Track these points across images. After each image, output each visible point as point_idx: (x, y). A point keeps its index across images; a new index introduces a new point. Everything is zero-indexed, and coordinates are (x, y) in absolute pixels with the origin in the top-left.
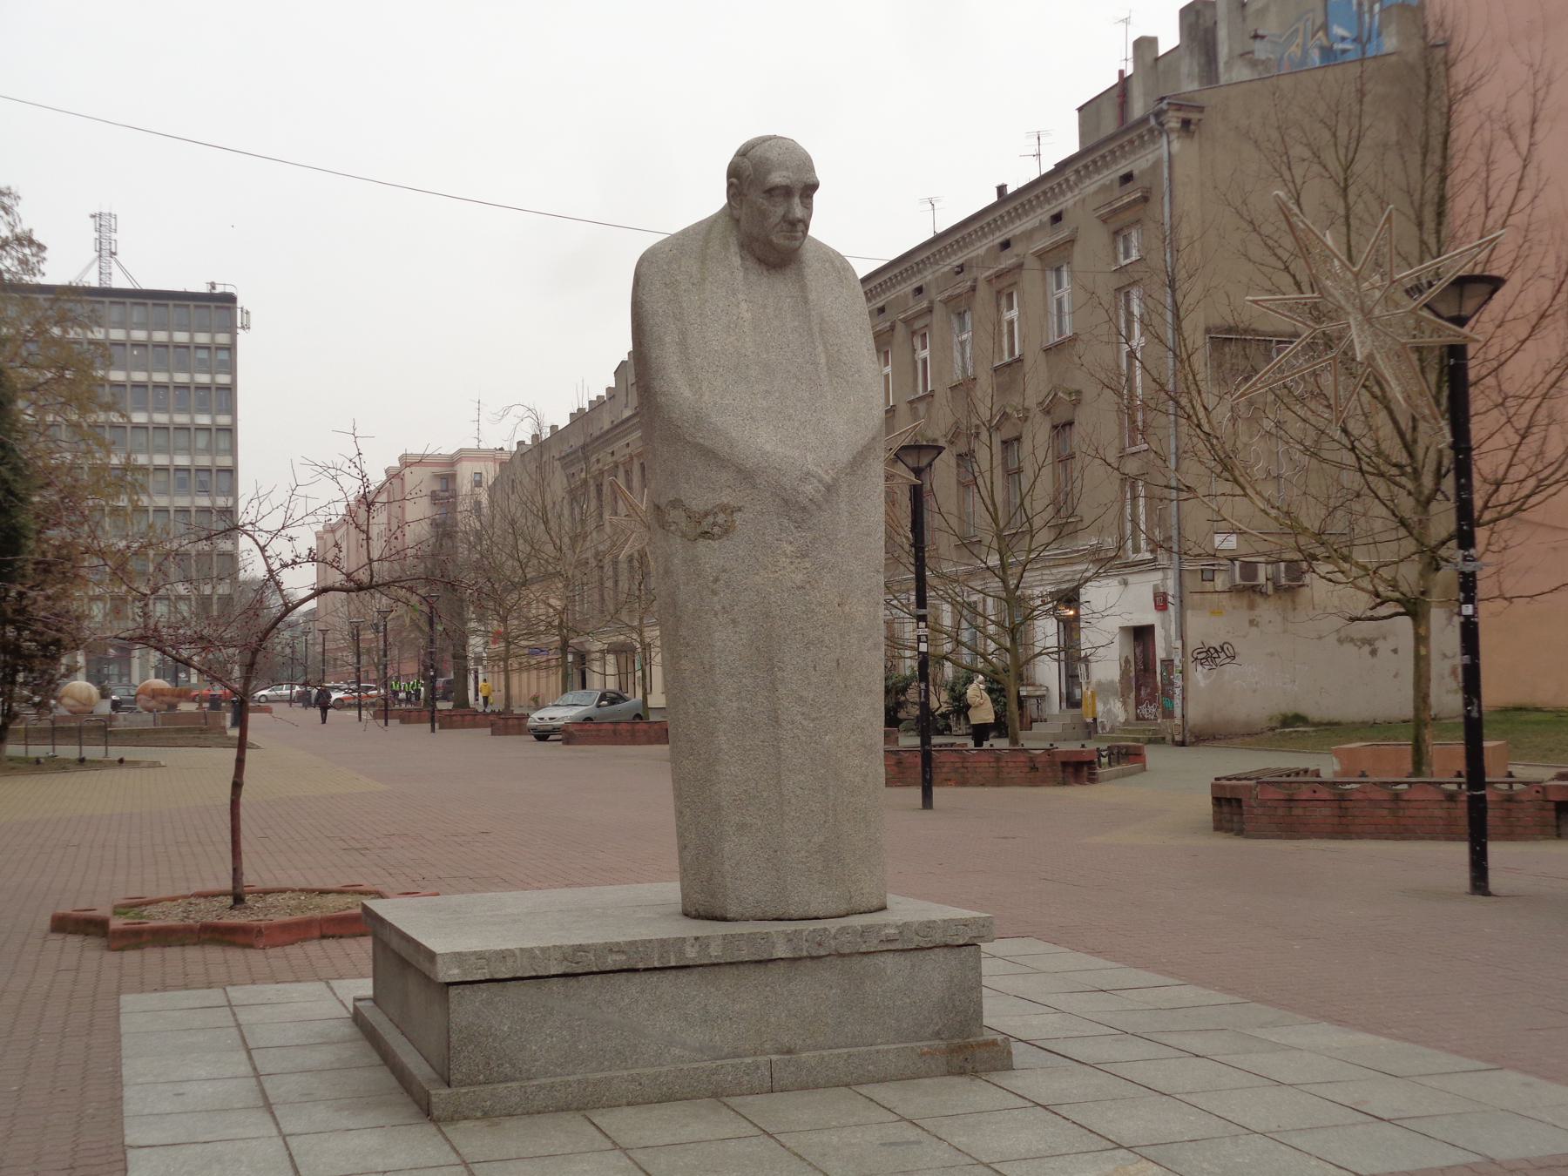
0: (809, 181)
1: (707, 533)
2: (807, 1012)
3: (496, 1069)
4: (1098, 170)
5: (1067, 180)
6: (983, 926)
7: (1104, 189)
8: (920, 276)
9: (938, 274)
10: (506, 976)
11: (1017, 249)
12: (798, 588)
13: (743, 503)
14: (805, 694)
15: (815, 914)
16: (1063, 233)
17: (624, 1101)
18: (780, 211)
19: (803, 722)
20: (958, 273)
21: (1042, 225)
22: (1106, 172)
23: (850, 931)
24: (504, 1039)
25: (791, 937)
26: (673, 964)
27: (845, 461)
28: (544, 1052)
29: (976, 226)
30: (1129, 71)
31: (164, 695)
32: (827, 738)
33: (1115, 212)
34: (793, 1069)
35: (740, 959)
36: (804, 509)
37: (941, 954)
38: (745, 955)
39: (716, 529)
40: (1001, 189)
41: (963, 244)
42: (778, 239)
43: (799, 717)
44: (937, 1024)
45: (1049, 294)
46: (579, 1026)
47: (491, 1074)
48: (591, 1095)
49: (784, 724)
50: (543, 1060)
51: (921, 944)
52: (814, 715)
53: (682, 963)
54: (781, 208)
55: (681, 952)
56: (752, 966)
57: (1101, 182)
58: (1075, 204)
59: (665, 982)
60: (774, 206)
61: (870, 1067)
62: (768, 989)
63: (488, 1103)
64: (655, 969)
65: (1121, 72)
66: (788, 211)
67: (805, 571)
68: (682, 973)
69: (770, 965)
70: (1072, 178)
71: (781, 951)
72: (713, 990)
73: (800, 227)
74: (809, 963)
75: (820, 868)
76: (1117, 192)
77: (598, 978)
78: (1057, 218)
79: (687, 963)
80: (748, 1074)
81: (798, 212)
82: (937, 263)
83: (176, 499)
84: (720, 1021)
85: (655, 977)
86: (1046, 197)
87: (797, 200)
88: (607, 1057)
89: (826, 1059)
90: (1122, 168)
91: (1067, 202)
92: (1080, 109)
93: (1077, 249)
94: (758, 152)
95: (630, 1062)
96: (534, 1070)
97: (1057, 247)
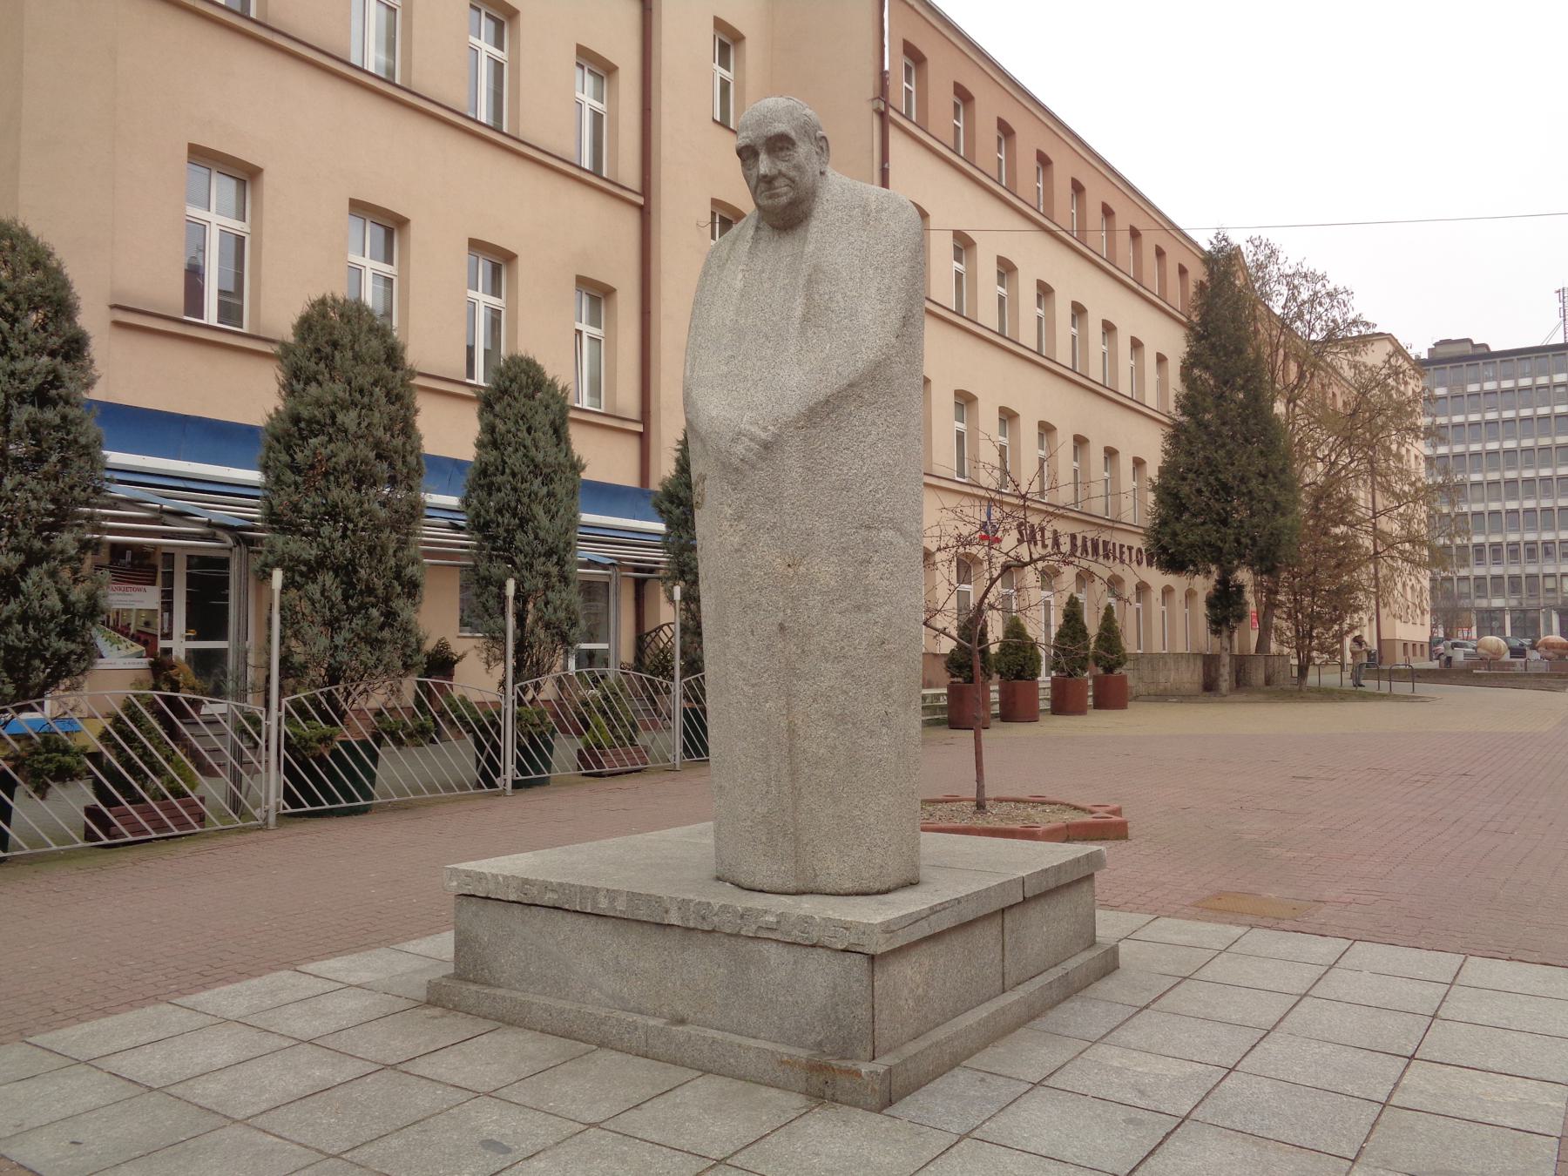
6: (864, 933)
15: (760, 887)
17: (539, 1027)
19: (746, 688)
26: (589, 911)
31: (1554, 648)
34: (664, 1039)
35: (638, 918)
36: (737, 469)
37: (825, 956)
38: (642, 914)
44: (819, 1033)
46: (531, 950)
49: (731, 689)
51: (799, 940)
52: (754, 682)
53: (594, 912)
55: (595, 902)
56: (654, 927)
59: (588, 927)
61: (732, 1060)
62: (666, 953)
64: (577, 912)
68: (600, 921)
69: (668, 930)
75: (764, 840)
77: (543, 911)
79: (598, 912)
80: (629, 1032)
83: (1542, 501)
85: (582, 920)
87: (763, 157)
89: (693, 1038)
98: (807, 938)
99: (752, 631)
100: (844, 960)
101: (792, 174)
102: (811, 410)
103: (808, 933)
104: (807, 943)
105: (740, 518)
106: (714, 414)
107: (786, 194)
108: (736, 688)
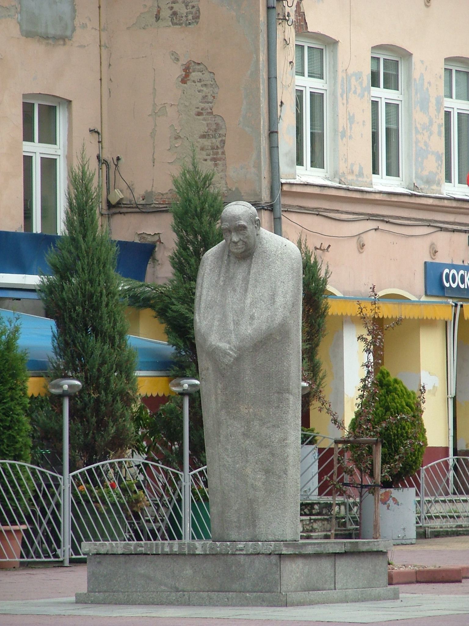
12: (224, 402)
19: (227, 459)
32: (237, 466)
43: (226, 456)
63: (93, 598)
74: (211, 557)
80: (181, 598)
99: (231, 435)
100: (270, 558)
101: (245, 240)
102: (255, 345)
106: (213, 343)
107: (243, 248)
108: (223, 458)
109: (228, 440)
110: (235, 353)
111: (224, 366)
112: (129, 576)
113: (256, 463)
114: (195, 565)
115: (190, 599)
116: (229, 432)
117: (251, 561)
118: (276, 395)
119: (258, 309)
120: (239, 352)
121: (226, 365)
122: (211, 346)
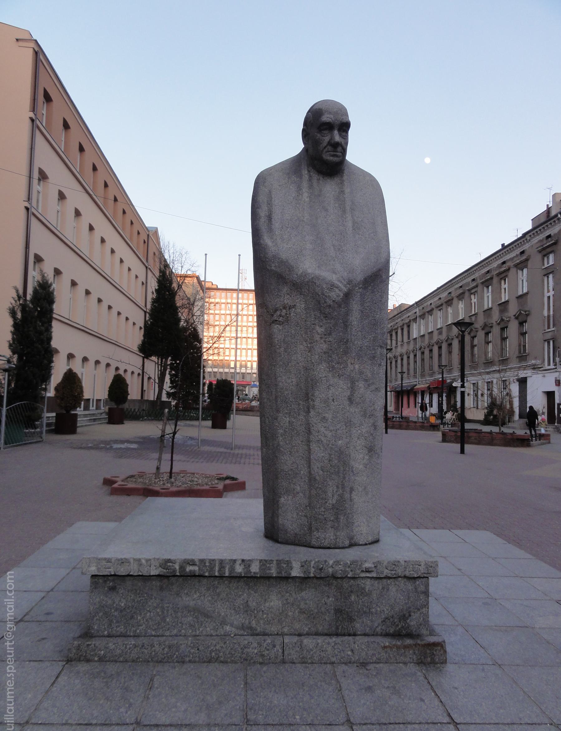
0: (344, 121)
1: (276, 321)
2: (312, 611)
3: (115, 629)
4: (538, 235)
5: (526, 239)
7: (541, 241)
8: (474, 275)
9: (480, 274)
10: (124, 574)
11: (508, 264)
12: (325, 353)
13: (295, 303)
14: (327, 415)
16: (524, 257)
17: (187, 659)
18: (327, 139)
19: (325, 432)
20: (487, 273)
21: (517, 255)
22: (541, 235)
23: (342, 563)
24: (121, 611)
25: (303, 564)
27: (358, 280)
28: (145, 621)
29: (494, 257)
30: (550, 205)
32: (340, 442)
33: (544, 249)
37: (403, 582)
39: (281, 319)
40: (503, 245)
41: (489, 264)
42: (327, 157)
45: (519, 278)
46: (168, 607)
47: (112, 631)
48: (167, 654)
50: (144, 626)
51: (389, 575)
54: (327, 138)
55: (232, 569)
57: (539, 239)
58: (529, 247)
60: (323, 136)
62: (288, 594)
63: (102, 652)
65: (548, 205)
66: (332, 138)
67: (329, 343)
70: (528, 238)
71: (296, 572)
72: (252, 592)
73: (339, 149)
76: (545, 241)
78: (522, 253)
80: (268, 650)
81: (337, 138)
82: (480, 270)
84: (256, 612)
86: (519, 246)
87: (336, 132)
88: (184, 627)
90: (547, 233)
91: (526, 247)
92: (532, 220)
93: (529, 262)
94: (315, 108)
95: (198, 632)
96: (138, 631)
97: (521, 262)
98: (395, 574)
99: (333, 400)
103: (396, 571)
104: (394, 576)
105: (330, 334)
106: (310, 271)
109: (328, 406)
110: (345, 286)
111: (329, 302)
112: (168, 611)
113: (358, 438)
114: (287, 592)
115: (286, 653)
116: (330, 395)
117: (383, 588)
118: (379, 349)
119: (361, 236)
120: (348, 286)
121: (333, 301)
122: (305, 274)
